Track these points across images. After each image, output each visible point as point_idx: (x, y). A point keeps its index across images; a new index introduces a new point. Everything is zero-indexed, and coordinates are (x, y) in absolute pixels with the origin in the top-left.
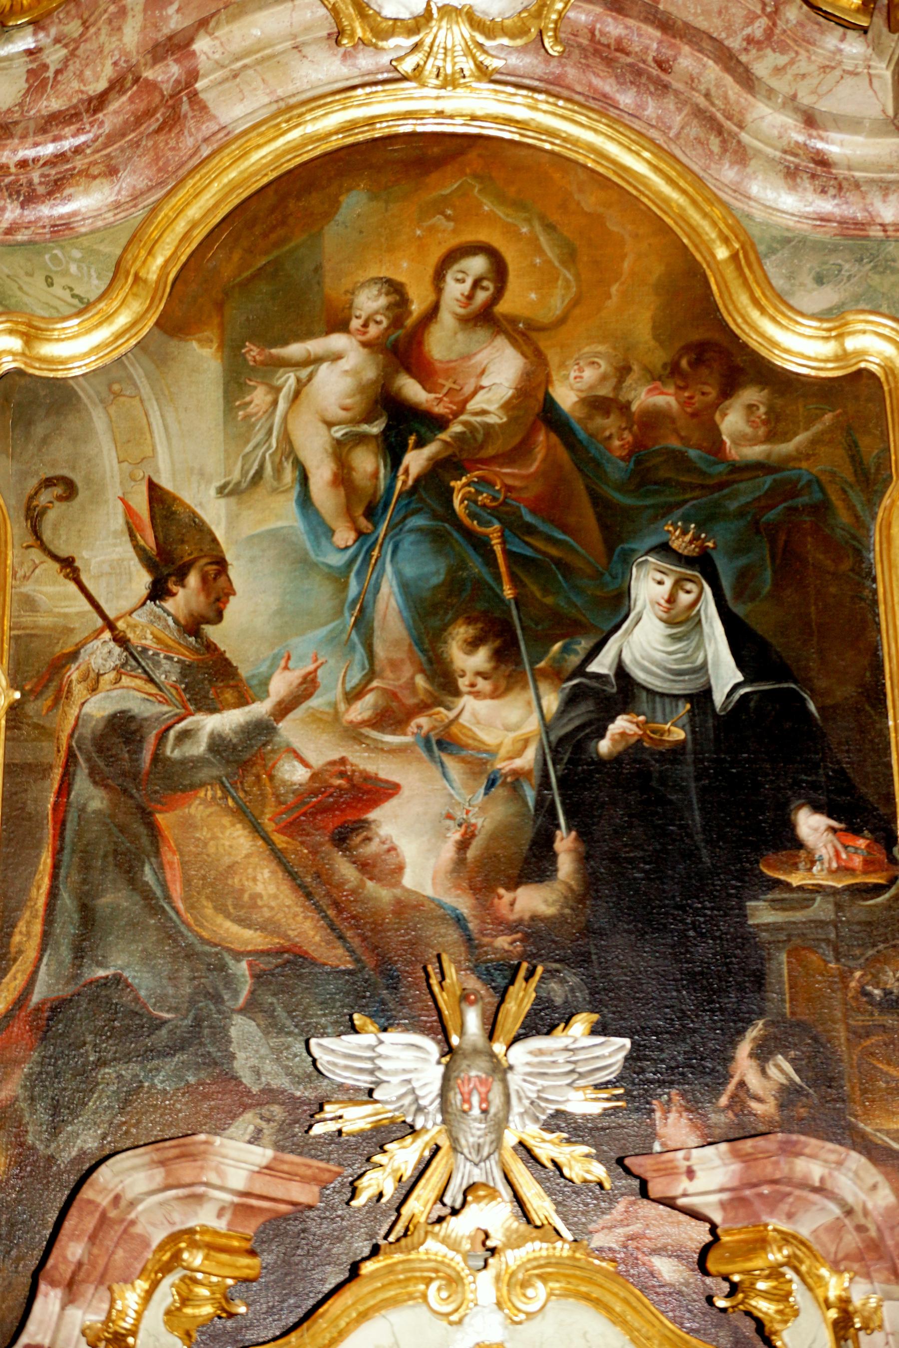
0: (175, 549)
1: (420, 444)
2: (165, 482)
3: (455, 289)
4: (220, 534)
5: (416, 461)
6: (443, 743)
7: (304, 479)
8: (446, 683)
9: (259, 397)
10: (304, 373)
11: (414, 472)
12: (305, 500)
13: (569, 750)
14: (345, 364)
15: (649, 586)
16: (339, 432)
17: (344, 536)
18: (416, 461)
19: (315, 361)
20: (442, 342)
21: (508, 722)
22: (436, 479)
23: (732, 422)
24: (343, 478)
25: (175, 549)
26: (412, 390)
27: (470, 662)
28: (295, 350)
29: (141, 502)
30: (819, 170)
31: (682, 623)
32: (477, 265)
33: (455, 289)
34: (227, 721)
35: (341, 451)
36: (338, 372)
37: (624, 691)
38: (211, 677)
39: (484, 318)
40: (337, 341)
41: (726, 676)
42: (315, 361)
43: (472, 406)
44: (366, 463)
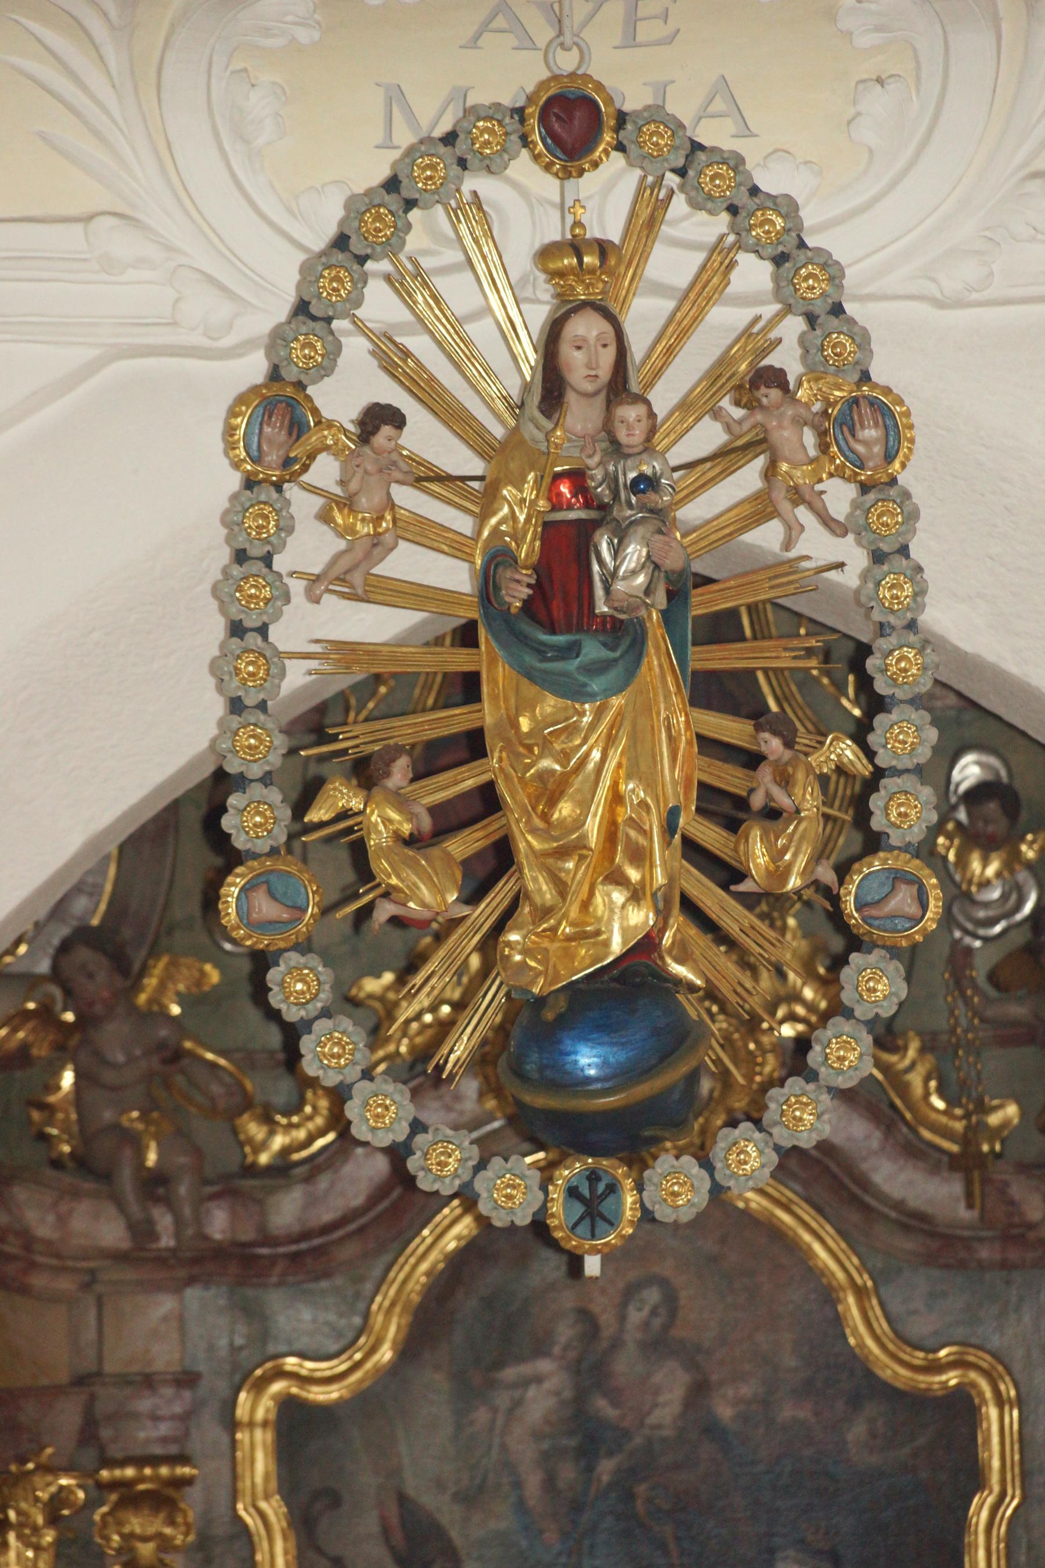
1: (610, 1454)
2: (411, 1492)
3: (635, 1316)
4: (454, 1534)
5: (606, 1468)
7: (518, 1485)
9: (482, 1415)
10: (517, 1394)
11: (606, 1479)
12: (521, 1506)
14: (547, 1385)
16: (545, 1445)
17: (551, 1536)
18: (606, 1468)
19: (525, 1383)
20: (625, 1365)
22: (624, 1486)
23: (857, 1432)
24: (550, 1482)
26: (602, 1406)
28: (510, 1373)
29: (393, 1511)
32: (653, 1295)
33: (635, 1316)
35: (547, 1460)
36: (540, 1388)
39: (658, 1345)
40: (544, 1366)
42: (525, 1383)
43: (652, 1420)
44: (568, 1473)
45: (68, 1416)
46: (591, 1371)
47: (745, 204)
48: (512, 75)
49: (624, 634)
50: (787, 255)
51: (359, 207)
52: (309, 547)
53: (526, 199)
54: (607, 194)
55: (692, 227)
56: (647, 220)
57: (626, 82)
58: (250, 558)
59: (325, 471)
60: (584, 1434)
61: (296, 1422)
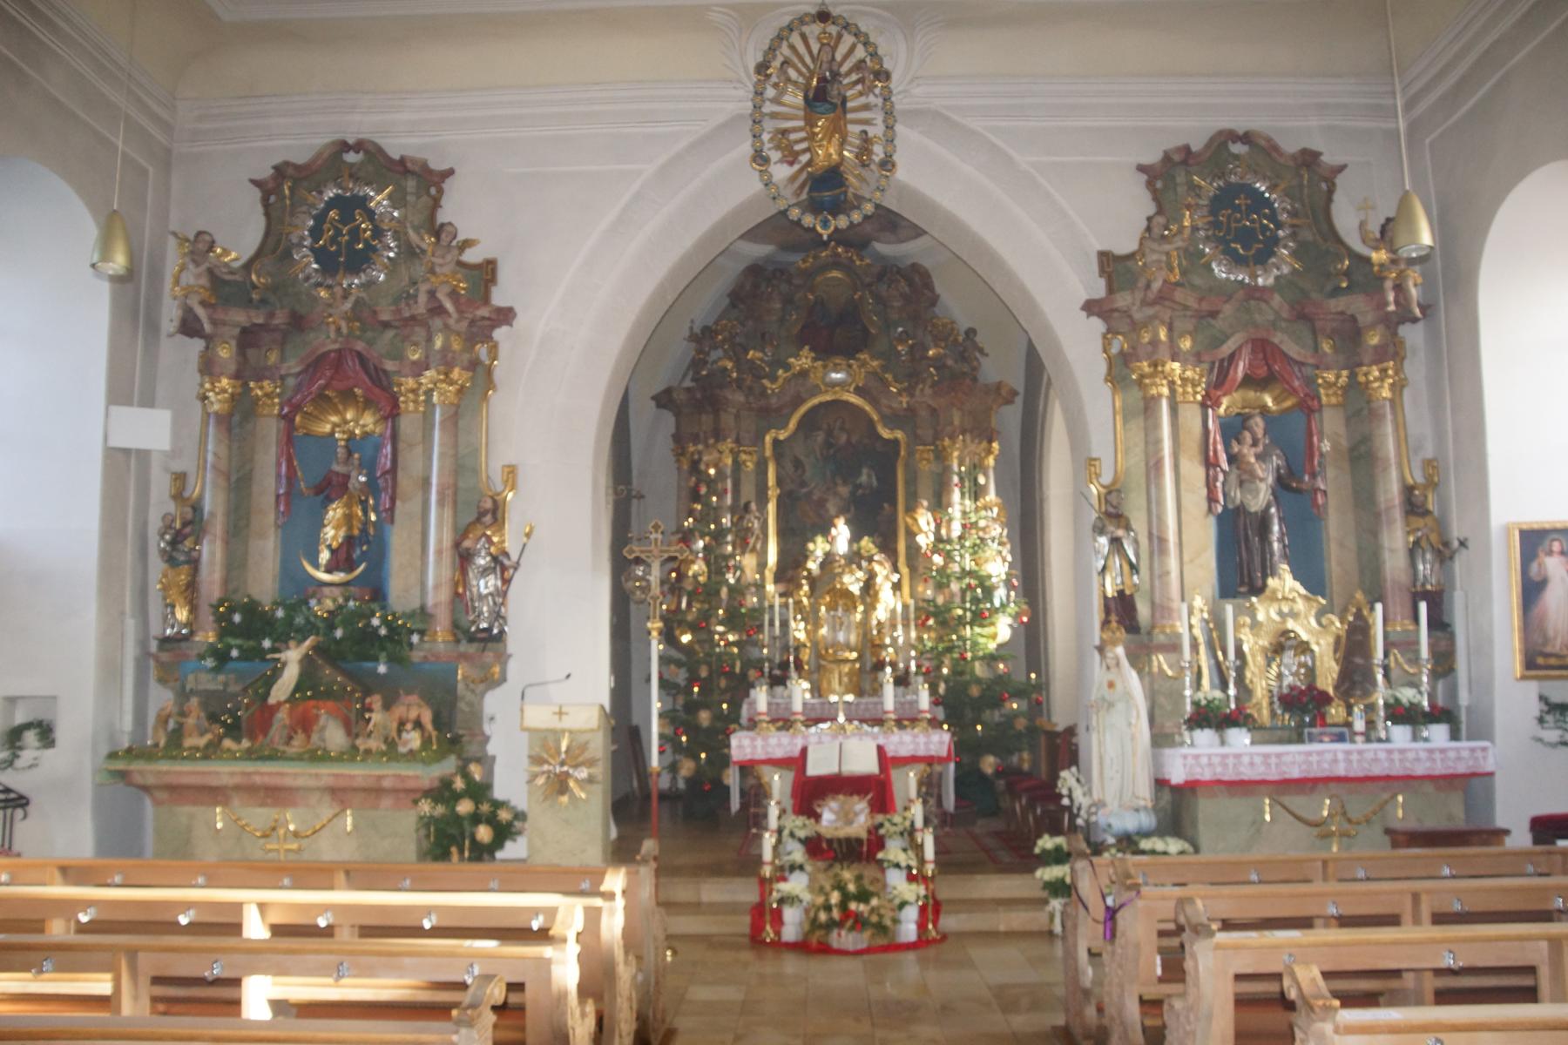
0: (798, 464)
6: (836, 494)
8: (836, 484)
13: (853, 494)
15: (865, 471)
21: (844, 490)
25: (798, 464)
27: (839, 481)
30: (890, 407)
31: (869, 476)
34: (804, 490)
36: (820, 437)
37: (860, 486)
38: (803, 484)
39: (842, 429)
41: (875, 483)
45: (734, 436)
46: (830, 433)
47: (857, 34)
48: (813, 11)
49: (835, 106)
50: (866, 44)
51: (782, 29)
52: (770, 92)
53: (813, 30)
54: (833, 30)
55: (848, 40)
56: (840, 36)
57: (835, 11)
58: (759, 93)
59: (774, 79)
60: (828, 444)
61: (776, 442)
